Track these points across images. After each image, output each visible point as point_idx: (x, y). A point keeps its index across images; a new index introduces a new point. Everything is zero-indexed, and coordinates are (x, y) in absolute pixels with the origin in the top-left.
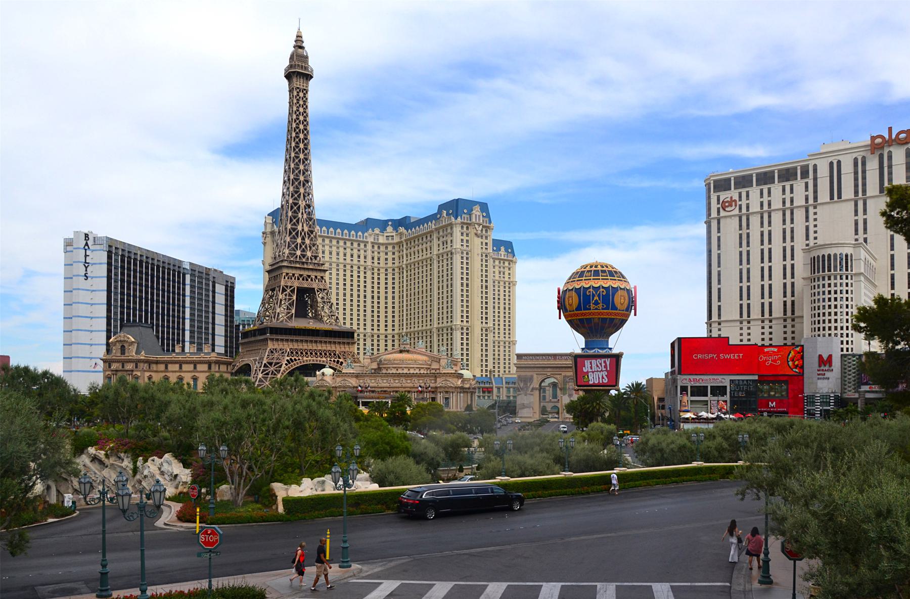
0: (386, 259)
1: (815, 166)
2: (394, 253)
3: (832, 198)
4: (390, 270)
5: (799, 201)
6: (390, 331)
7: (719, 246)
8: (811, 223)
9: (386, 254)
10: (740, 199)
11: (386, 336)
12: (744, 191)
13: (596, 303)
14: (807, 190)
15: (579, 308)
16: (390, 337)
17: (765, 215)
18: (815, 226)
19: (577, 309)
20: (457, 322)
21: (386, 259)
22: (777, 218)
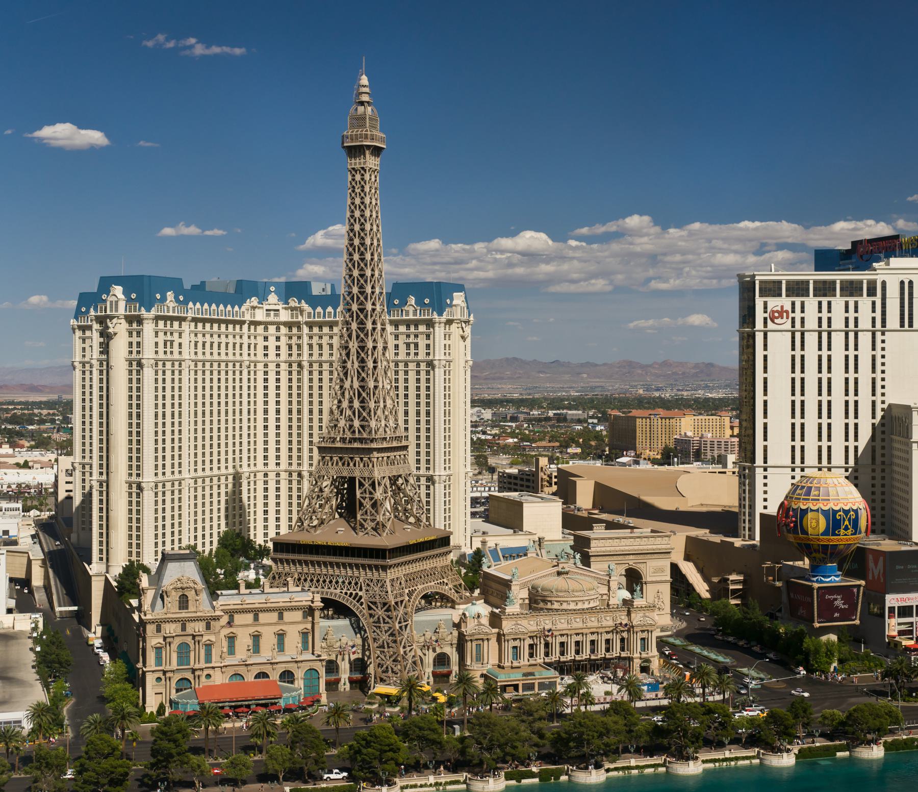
0: (266, 348)
1: (884, 284)
2: (278, 339)
3: (902, 325)
4: (272, 367)
5: (865, 323)
6: (272, 466)
7: (765, 368)
8: (879, 353)
9: (266, 339)
10: (793, 312)
11: (266, 475)
12: (798, 301)
13: (846, 528)
14: (874, 311)
15: (826, 533)
16: (272, 476)
17: (825, 334)
18: (883, 357)
19: (822, 534)
20: (439, 471)
21: (266, 348)
22: (838, 339)
